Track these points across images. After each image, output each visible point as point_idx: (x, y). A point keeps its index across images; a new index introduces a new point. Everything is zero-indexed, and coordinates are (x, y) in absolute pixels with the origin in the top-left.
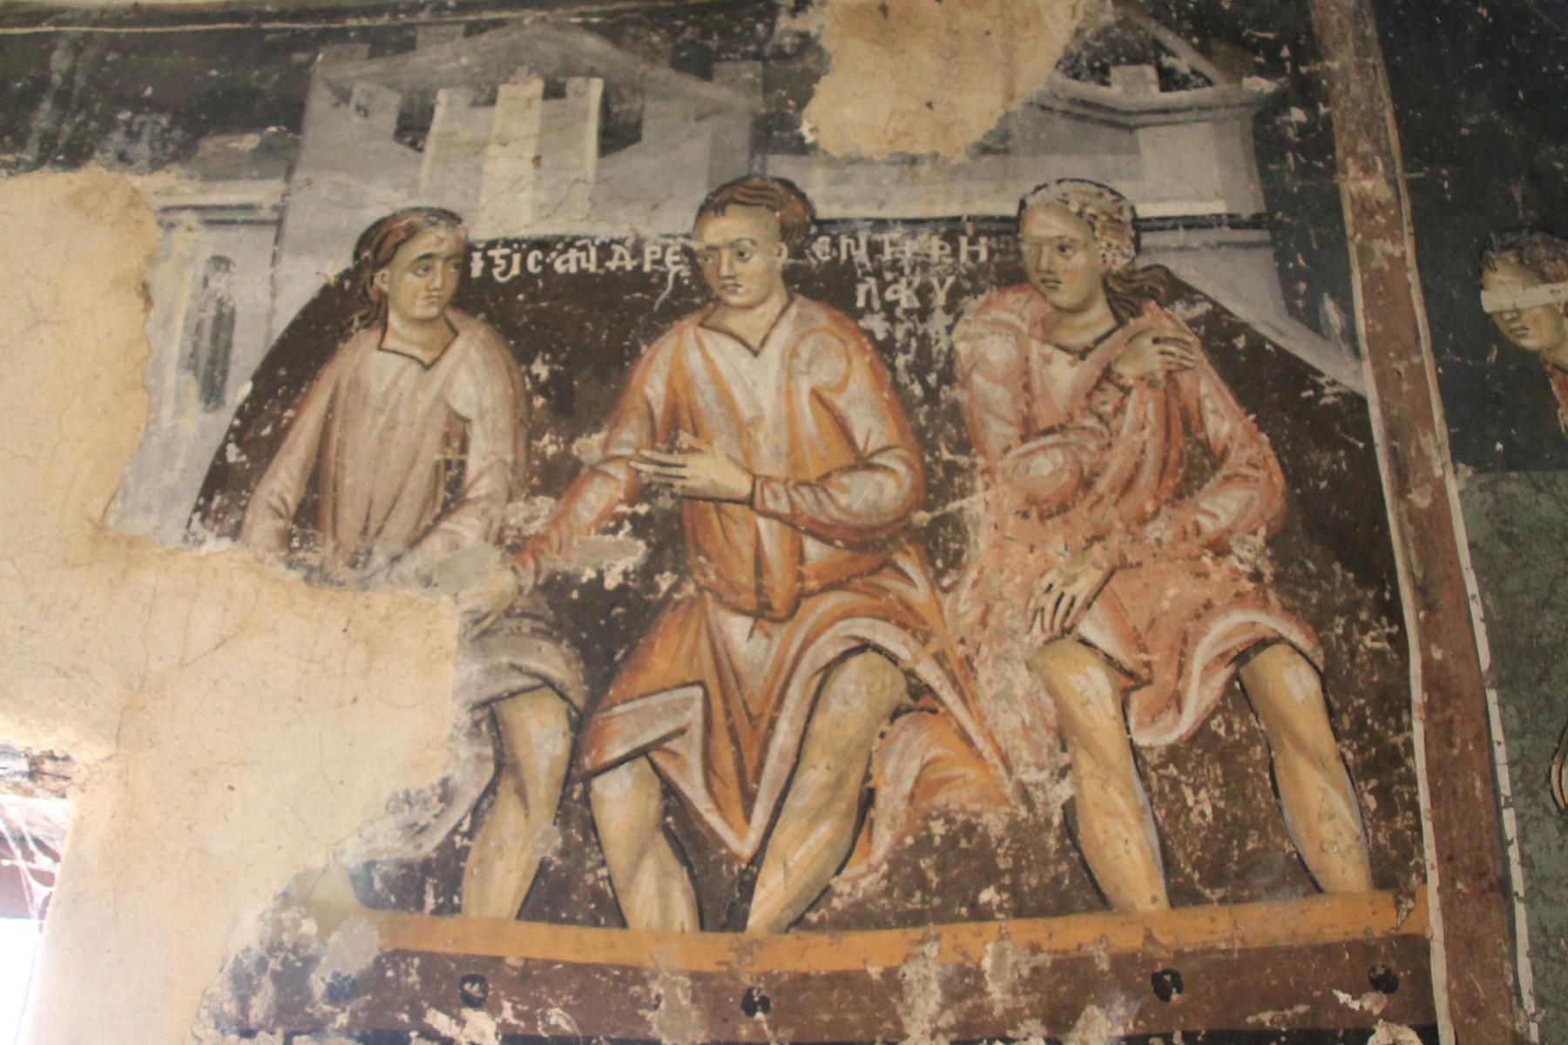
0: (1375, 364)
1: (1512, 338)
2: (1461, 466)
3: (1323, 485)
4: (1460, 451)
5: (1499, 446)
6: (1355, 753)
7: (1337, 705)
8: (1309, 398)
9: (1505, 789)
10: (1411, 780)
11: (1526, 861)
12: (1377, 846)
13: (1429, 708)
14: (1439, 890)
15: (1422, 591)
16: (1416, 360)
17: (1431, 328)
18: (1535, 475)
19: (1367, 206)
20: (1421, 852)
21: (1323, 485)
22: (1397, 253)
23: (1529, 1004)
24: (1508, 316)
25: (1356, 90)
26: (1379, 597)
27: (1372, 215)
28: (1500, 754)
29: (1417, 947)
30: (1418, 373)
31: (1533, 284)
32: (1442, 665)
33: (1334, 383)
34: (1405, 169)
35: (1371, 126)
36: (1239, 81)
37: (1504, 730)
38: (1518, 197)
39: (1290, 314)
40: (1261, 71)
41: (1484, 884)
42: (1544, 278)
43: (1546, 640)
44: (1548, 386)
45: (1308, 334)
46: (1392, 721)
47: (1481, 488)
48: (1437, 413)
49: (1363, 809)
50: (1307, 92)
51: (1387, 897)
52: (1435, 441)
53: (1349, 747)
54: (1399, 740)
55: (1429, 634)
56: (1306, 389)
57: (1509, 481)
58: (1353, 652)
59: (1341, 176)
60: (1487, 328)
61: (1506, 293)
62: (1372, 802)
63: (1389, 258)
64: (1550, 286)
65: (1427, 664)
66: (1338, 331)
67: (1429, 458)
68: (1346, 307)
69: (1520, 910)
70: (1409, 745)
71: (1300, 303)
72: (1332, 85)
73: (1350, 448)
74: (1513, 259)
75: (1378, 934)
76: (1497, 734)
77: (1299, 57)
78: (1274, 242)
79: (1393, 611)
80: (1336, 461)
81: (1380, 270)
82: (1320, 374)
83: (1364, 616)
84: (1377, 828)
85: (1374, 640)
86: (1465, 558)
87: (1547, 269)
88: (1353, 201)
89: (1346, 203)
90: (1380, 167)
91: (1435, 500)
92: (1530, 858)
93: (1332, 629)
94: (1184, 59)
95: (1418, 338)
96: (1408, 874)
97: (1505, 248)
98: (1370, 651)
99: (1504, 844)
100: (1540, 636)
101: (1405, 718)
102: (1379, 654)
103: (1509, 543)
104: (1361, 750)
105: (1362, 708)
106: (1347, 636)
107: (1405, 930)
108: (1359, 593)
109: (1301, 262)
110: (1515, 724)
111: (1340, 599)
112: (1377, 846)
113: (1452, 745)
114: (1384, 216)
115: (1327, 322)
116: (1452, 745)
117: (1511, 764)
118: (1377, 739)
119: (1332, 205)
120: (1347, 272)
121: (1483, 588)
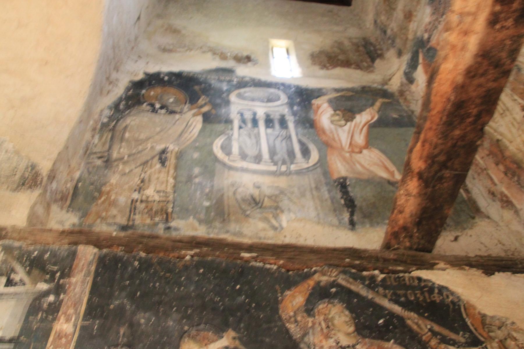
25: (78, 289)
27: (61, 339)
34: (83, 320)
35: (76, 305)
36: (36, 284)
40: (46, 281)
50: (59, 290)
72: (69, 287)
77: (62, 277)
94: (20, 274)
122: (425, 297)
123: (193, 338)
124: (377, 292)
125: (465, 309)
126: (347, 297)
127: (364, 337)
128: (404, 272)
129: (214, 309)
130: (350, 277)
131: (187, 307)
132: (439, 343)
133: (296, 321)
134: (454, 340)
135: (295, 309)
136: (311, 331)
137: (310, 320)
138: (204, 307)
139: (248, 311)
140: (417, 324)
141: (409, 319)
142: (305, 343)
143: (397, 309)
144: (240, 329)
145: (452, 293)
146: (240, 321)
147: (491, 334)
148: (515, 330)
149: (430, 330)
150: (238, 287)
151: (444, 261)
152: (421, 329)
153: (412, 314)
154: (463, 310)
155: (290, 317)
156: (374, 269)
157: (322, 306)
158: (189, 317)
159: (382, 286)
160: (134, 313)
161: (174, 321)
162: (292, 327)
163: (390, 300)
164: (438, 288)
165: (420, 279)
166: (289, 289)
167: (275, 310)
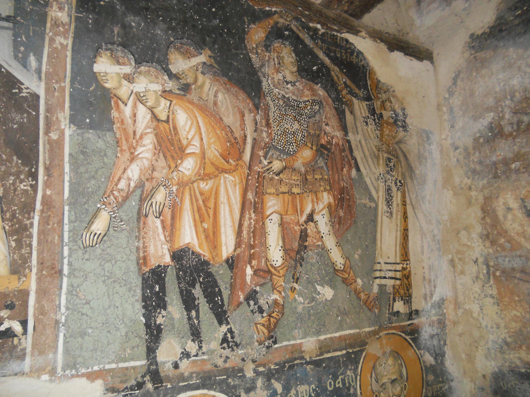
0: (46, 84)
1: (102, 82)
2: (72, 126)
3: (15, 126)
4: (73, 120)
5: (88, 120)
6: (9, 226)
7: (5, 209)
8: (16, 92)
9: (66, 239)
10: (31, 236)
11: (70, 264)
12: (14, 260)
13: (42, 211)
14: (36, 274)
15: (47, 169)
16: (63, 85)
17: (72, 74)
18: (98, 132)
19: (57, 23)
20: (31, 262)
21: (15, 126)
22: (65, 44)
23: (63, 309)
24: (102, 74)
26: (30, 170)
27: (58, 26)
28: (66, 228)
29: (24, 294)
30: (63, 89)
31: (114, 65)
32: (50, 196)
33: (28, 88)
34: (76, 12)
37: (69, 219)
38: (116, 32)
39: (15, 59)
41: (53, 271)
42: (119, 63)
43: (90, 190)
44: (110, 101)
45: (21, 68)
46: (26, 215)
47: (78, 135)
48: (67, 105)
49: (9, 246)
51: (15, 277)
52: (64, 117)
53: (7, 224)
54: (28, 222)
55: (47, 185)
56: (15, 89)
57: (89, 133)
58: (15, 190)
59: (50, 9)
60: (94, 76)
61: (105, 66)
62: (13, 244)
63: (61, 44)
64: (120, 66)
65: (44, 196)
66: (34, 69)
67: (60, 121)
68: (39, 60)
69: (65, 280)
70: (32, 224)
71: (20, 55)
73: (29, 113)
74: (109, 54)
75: (10, 289)
76: (66, 221)
78: (13, 29)
79: (34, 176)
80: (23, 118)
81: (56, 48)
82: (23, 84)
83: (22, 177)
84: (14, 253)
85: (24, 186)
86: (67, 158)
87: (120, 60)
88: (52, 19)
89: (49, 19)
90: (66, 9)
91: (60, 137)
92: (71, 263)
93: (8, 181)
95: (65, 76)
96: (25, 269)
97: (107, 50)
98: (23, 190)
99: (63, 258)
100: (88, 188)
101: (32, 215)
102: (27, 191)
103: (83, 155)
104: (12, 226)
105: (15, 210)
106: (14, 184)
107: (21, 288)
108: (22, 168)
109: (24, 39)
110: (73, 218)
111: (13, 170)
112: (14, 260)
113: (48, 224)
114: (63, 28)
115: (30, 64)
116: (48, 224)
117: (70, 231)
118: (20, 222)
119: (43, 19)
120: (43, 46)
121: (71, 170)
122: (347, 57)
123: (178, 49)
124: (317, 43)
125: (369, 73)
126: (296, 41)
127: (302, 77)
128: (337, 31)
129: (194, 26)
130: (300, 25)
131: (171, 19)
132: (347, 94)
133: (257, 53)
134: (357, 94)
135: (257, 42)
136: (267, 64)
137: (267, 54)
138: (185, 22)
139: (221, 35)
140: (337, 76)
141: (333, 71)
142: (262, 72)
143: (327, 61)
144: (214, 50)
145: (365, 59)
146: (214, 43)
147: (379, 95)
148: (393, 96)
149: (345, 83)
150: (214, 10)
151: (366, 30)
152: (339, 80)
153: (336, 67)
154: (368, 73)
155: (253, 48)
156: (318, 23)
157: (276, 44)
158: (173, 29)
159: (321, 39)
160: (124, 14)
161: (161, 30)
162: (253, 57)
163: (324, 53)
164: (357, 52)
165: (347, 41)
166: (254, 23)
167: (242, 40)
